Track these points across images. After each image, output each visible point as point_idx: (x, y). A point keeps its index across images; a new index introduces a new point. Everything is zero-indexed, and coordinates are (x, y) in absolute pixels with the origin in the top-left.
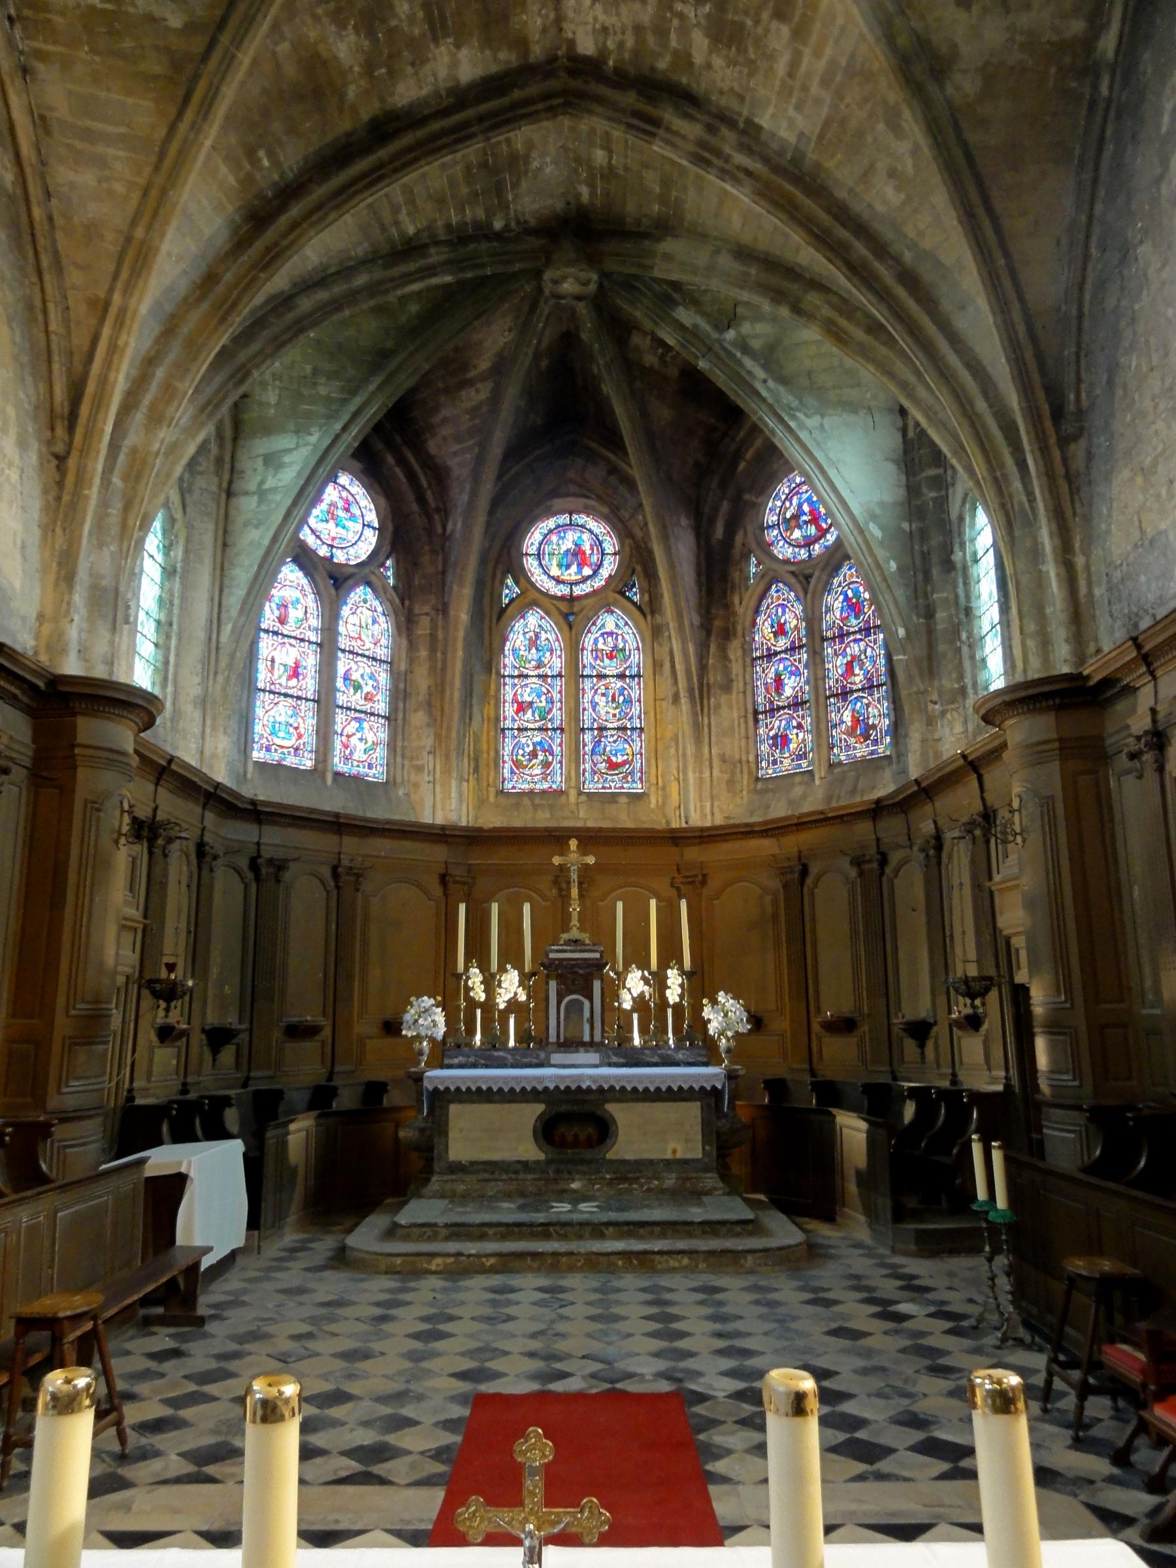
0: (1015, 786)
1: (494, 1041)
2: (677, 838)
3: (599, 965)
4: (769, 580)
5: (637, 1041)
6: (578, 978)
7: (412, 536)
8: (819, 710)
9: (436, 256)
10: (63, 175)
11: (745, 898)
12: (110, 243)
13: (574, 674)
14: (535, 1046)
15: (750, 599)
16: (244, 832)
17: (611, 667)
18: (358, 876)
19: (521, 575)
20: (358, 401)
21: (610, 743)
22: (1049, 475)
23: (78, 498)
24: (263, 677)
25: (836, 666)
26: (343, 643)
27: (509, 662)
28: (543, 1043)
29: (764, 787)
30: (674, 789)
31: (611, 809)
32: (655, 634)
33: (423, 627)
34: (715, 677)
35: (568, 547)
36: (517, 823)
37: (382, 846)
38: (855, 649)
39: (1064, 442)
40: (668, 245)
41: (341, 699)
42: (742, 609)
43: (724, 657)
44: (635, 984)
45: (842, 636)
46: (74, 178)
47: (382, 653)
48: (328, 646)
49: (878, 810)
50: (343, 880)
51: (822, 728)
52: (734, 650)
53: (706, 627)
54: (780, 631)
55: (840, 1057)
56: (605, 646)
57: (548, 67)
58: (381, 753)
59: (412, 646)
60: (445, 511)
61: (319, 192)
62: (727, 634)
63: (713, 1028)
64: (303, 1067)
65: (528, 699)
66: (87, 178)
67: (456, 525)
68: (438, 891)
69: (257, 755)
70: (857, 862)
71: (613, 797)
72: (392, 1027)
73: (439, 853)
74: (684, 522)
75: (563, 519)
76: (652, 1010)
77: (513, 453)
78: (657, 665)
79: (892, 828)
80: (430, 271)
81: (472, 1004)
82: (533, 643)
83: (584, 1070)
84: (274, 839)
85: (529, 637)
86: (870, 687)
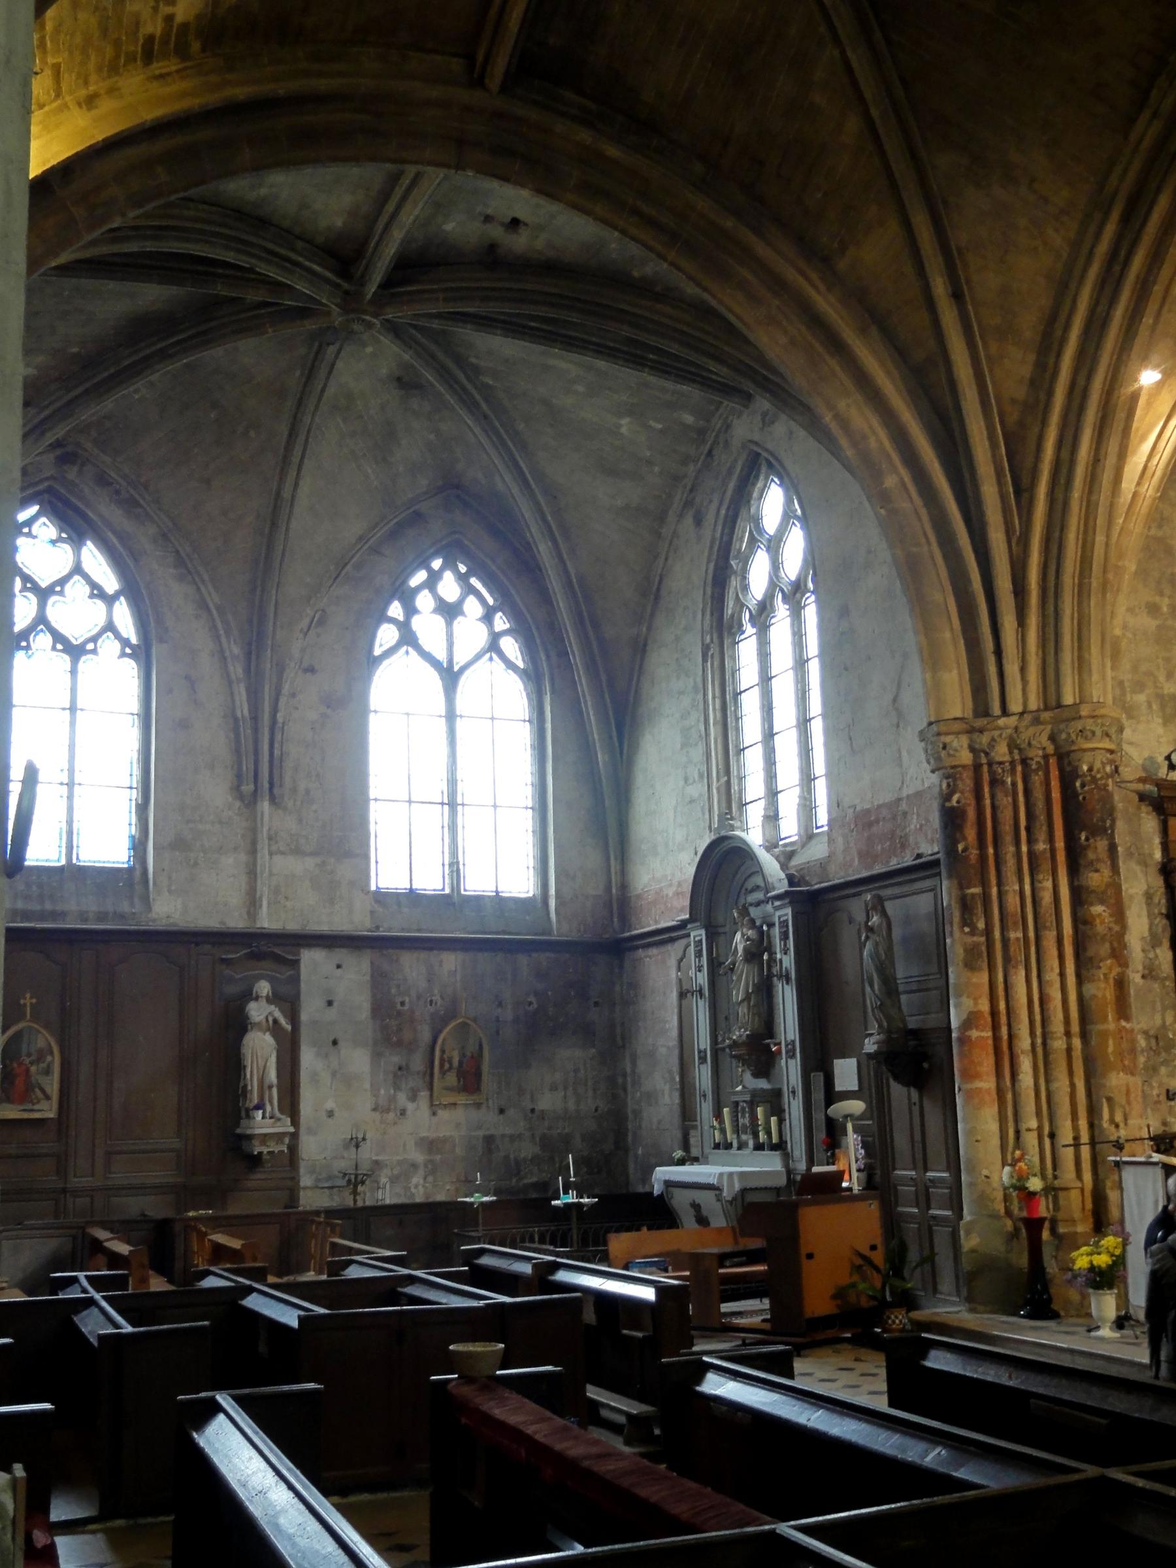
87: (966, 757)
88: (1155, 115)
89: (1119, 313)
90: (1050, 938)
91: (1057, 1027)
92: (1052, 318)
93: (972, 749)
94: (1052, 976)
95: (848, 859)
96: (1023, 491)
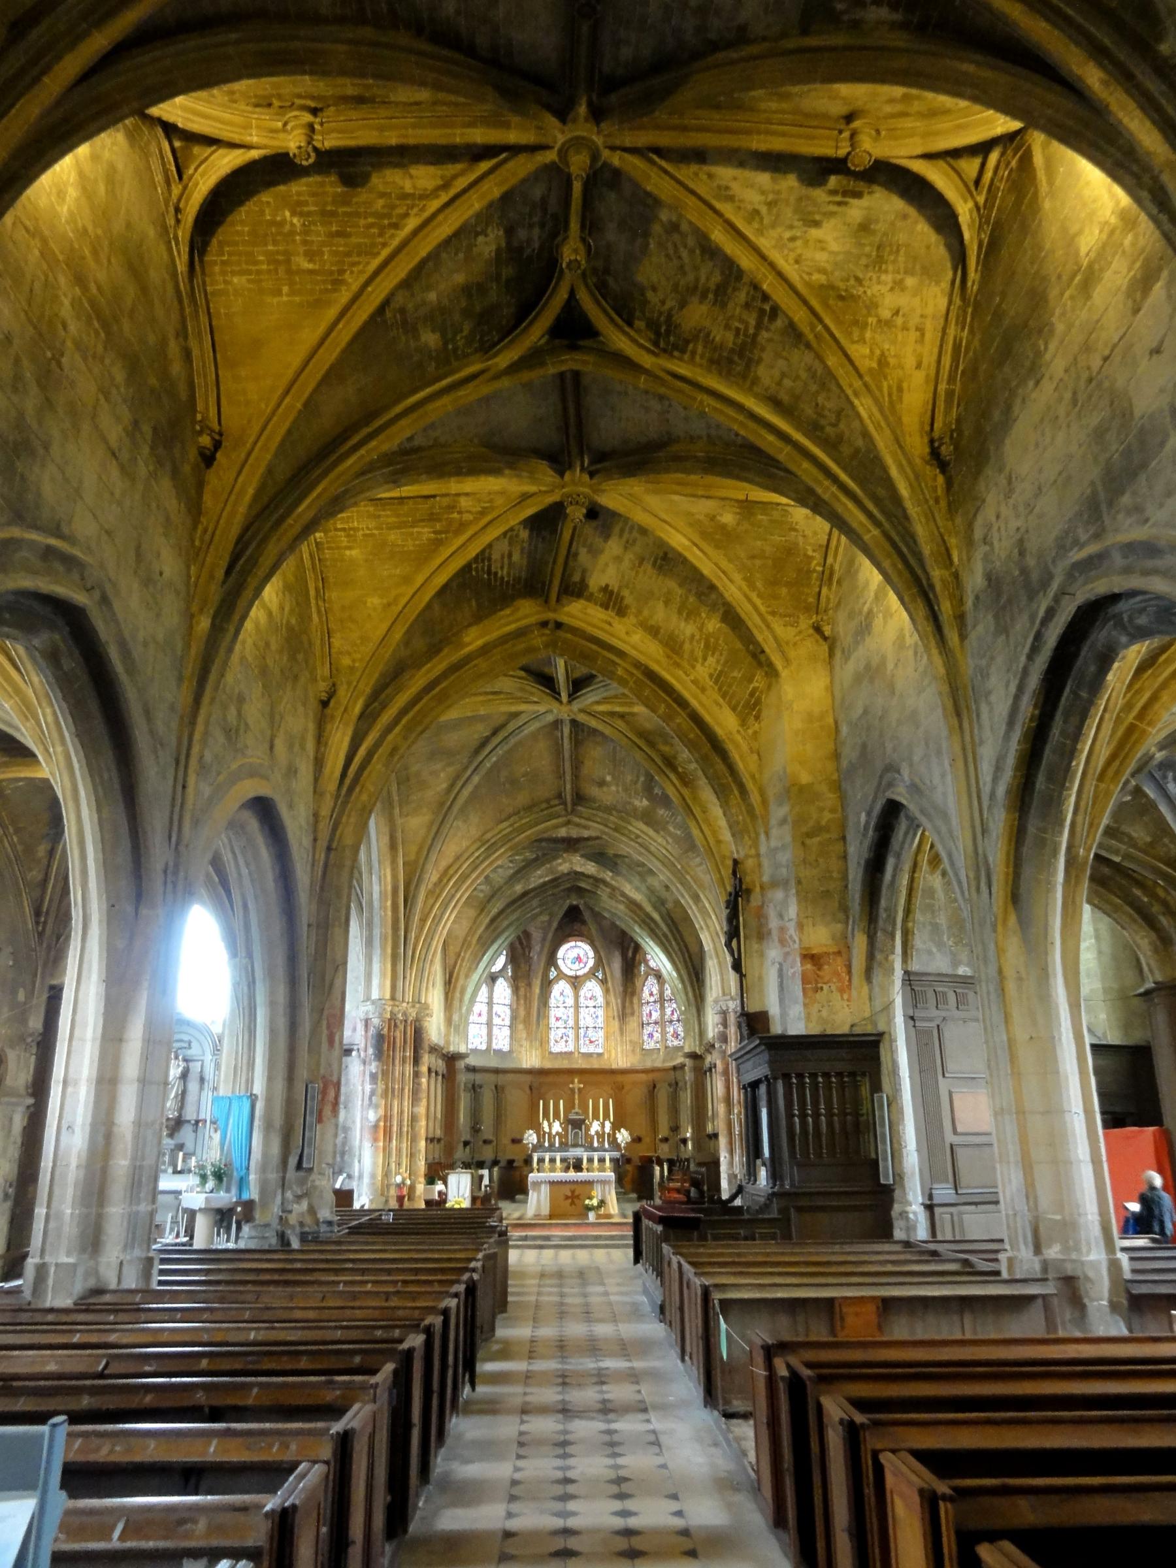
0: (689, 1076)
1: (552, 1145)
2: (613, 1072)
4: (647, 975)
5: (596, 1144)
6: (578, 1124)
7: (519, 956)
8: (660, 1029)
11: (635, 1096)
13: (577, 1006)
14: (564, 1146)
15: (641, 979)
16: (471, 1076)
17: (591, 1003)
18: (503, 1088)
19: (557, 968)
21: (590, 1032)
24: (472, 1018)
25: (668, 1011)
28: (566, 1144)
32: (607, 991)
33: (522, 992)
34: (628, 1011)
35: (575, 955)
37: (510, 1077)
42: (638, 984)
43: (631, 1003)
44: (595, 1127)
47: (508, 1002)
48: (490, 1004)
49: (675, 1068)
51: (664, 1033)
52: (635, 1000)
53: (625, 992)
54: (651, 994)
55: (664, 1151)
62: (633, 993)
67: (534, 954)
71: (590, 1055)
72: (517, 1141)
73: (528, 1078)
75: (573, 944)
76: (600, 1135)
78: (608, 1003)
79: (678, 1073)
85: (560, 991)
89: (474, 876)
96: (423, 921)
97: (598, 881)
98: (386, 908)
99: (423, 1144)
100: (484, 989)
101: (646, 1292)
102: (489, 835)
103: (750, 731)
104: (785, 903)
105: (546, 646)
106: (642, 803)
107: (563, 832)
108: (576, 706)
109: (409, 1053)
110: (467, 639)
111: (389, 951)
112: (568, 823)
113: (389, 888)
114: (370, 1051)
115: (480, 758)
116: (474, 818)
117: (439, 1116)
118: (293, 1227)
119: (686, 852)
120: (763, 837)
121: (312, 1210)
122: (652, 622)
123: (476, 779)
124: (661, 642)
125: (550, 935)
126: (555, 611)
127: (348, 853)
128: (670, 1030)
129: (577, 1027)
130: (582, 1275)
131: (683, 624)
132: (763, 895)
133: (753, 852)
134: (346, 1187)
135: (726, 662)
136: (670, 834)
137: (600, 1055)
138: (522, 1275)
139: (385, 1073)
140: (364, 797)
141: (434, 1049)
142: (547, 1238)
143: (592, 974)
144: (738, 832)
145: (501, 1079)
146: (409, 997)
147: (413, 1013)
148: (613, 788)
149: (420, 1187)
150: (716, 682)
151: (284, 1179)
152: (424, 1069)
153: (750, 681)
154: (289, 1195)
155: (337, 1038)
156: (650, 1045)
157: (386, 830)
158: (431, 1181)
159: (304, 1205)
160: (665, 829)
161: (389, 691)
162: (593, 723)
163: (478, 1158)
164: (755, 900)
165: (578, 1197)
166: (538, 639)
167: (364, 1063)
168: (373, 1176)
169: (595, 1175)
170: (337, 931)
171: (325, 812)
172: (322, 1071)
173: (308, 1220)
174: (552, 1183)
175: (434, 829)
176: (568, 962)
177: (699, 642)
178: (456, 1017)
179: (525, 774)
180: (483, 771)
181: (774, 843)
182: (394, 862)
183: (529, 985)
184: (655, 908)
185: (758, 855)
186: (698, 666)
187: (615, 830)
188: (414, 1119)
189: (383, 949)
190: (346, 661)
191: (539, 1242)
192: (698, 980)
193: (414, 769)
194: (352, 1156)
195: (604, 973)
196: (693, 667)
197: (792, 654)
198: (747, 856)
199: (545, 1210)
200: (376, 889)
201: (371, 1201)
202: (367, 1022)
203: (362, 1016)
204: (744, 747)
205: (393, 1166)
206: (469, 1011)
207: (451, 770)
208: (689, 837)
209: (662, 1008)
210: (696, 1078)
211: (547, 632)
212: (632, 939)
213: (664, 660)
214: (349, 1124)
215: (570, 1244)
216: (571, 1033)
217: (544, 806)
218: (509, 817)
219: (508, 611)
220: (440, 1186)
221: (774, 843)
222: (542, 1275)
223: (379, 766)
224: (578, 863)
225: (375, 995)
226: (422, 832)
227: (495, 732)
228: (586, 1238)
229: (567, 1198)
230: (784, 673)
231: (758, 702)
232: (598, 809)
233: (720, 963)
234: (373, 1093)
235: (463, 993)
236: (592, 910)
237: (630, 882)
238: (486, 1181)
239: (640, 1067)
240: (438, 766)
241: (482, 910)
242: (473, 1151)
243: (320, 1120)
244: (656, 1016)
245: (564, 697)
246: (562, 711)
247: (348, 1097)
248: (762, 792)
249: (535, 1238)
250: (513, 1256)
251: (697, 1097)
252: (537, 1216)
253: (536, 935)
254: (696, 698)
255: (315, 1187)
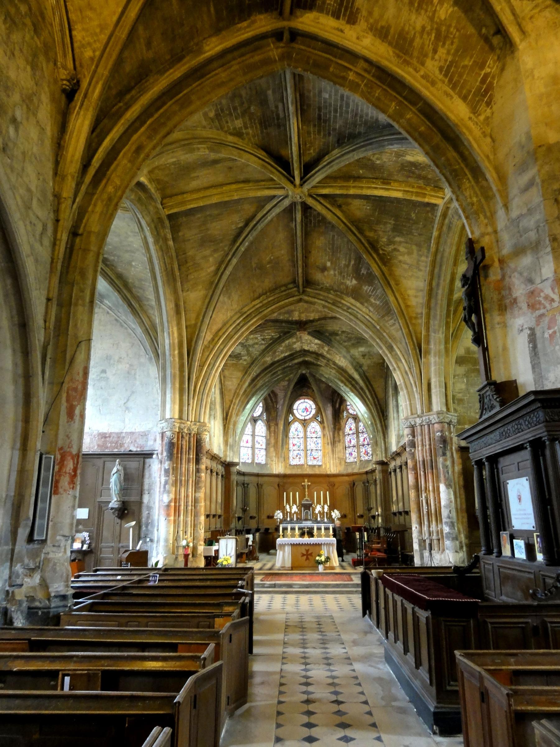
0: (378, 476)
1: (292, 520)
3: (311, 505)
4: (348, 418)
5: (319, 519)
6: (307, 507)
8: (357, 450)
9: (279, 373)
10: (227, 383)
11: (342, 490)
12: (233, 392)
13: (306, 437)
14: (299, 520)
15: (344, 421)
16: (241, 478)
17: (314, 435)
18: (262, 485)
19: (293, 414)
20: (262, 392)
21: (314, 453)
22: (382, 426)
23: (228, 431)
24: (242, 444)
25: (361, 439)
26: (256, 434)
27: (291, 435)
28: (301, 519)
29: (348, 464)
30: (328, 464)
31: (314, 469)
32: (324, 428)
34: (336, 439)
35: (304, 407)
36: (294, 473)
37: (266, 479)
38: (365, 436)
39: (384, 421)
40: (322, 368)
41: (256, 446)
42: (342, 423)
44: (318, 509)
45: (363, 432)
46: (228, 383)
47: (264, 435)
48: (253, 435)
49: (367, 473)
50: (259, 486)
51: (359, 452)
52: (341, 433)
53: (335, 428)
54: (351, 429)
55: (361, 523)
56: (313, 430)
57: (300, 351)
58: (264, 458)
59: (270, 433)
60: (277, 402)
61: (262, 375)
62: (339, 429)
63: (333, 517)
64: (253, 525)
65: (295, 443)
66: (230, 383)
67: (279, 406)
68: (277, 487)
69: (241, 461)
70: (364, 483)
71: (314, 466)
72: (271, 517)
73: (277, 480)
74: (329, 405)
75: (302, 401)
76: (322, 514)
77: (292, 393)
78: (324, 435)
79: (369, 476)
80: (278, 375)
81: (287, 512)
82: (296, 430)
83: (309, 524)
84: (247, 479)
85: (295, 428)
86: (368, 445)
87: (177, 430)
88: (261, 302)
89: (236, 337)
90: (191, 480)
91: (190, 503)
92: (220, 330)
93: (179, 428)
94: (190, 490)
95: (91, 446)
96: (201, 366)
97: (318, 355)
98: (174, 356)
99: (202, 518)
100: (249, 426)
101: (388, 659)
102: (246, 309)
103: (482, 118)
104: (536, 267)
105: (282, 57)
106: (352, 283)
107: (296, 316)
108: (306, 187)
109: (192, 456)
110: (207, 48)
111: (177, 385)
112: (300, 300)
113: (176, 341)
114: (165, 454)
115: (238, 244)
116: (235, 297)
117: (219, 500)
118: (20, 603)
119: (383, 317)
120: (501, 213)
121: (44, 585)
122: (383, 23)
123: (235, 261)
124: (390, 44)
125: (289, 393)
126: (289, 20)
127: (93, 239)
128: (363, 450)
129: (306, 450)
130: (319, 624)
131: (413, 17)
132: (502, 269)
133: (490, 229)
134: (144, 549)
135: (457, 51)
136: (372, 305)
137: (320, 466)
138: (271, 626)
139: (175, 470)
140: (110, 189)
141: (214, 457)
142: (290, 586)
143: (315, 418)
144: (471, 214)
145: (261, 480)
146: (192, 417)
147: (195, 429)
148: (332, 272)
149: (201, 548)
150: (446, 75)
151: (13, 551)
152: (203, 467)
153: (482, 67)
154: (18, 568)
155: (77, 412)
156: (350, 459)
157: (171, 297)
158: (210, 542)
159: (37, 578)
160: (367, 301)
161: (133, 92)
162: (319, 208)
163: (247, 527)
164: (494, 275)
165: (311, 554)
166: (274, 51)
167: (161, 462)
168: (167, 540)
169: (323, 539)
170: (81, 311)
171: (67, 192)
172: (60, 443)
173: (40, 595)
174: (293, 545)
175: (207, 300)
176: (300, 411)
177: (429, 34)
178: (230, 440)
179: (270, 262)
180: (239, 254)
181: (514, 214)
182: (179, 324)
183: (277, 425)
184: (356, 370)
185: (495, 232)
186: (429, 63)
187: (333, 304)
188: (196, 501)
189: (173, 384)
190: (88, 53)
191: (284, 589)
192: (383, 415)
193: (190, 253)
194: (153, 526)
195: (322, 418)
196: (423, 64)
197: (529, 27)
198: (483, 235)
199: (288, 564)
200: (167, 341)
201: (165, 558)
202: (163, 434)
203: (160, 430)
204: (477, 132)
205: (181, 533)
206: (240, 439)
207: (218, 256)
208: (387, 303)
209: (358, 437)
210: (384, 478)
211: (282, 45)
212: (339, 394)
213: (394, 59)
214: (151, 504)
215: (306, 590)
216: (302, 453)
217: (283, 289)
218: (258, 298)
219: (245, 24)
220: (215, 547)
221: (514, 214)
222: (287, 627)
223: (125, 161)
224: (307, 342)
225: (168, 416)
226: (199, 303)
227: (246, 225)
228: (318, 586)
229: (303, 555)
230: (521, 46)
231: (490, 87)
232: (321, 289)
233: (408, 392)
234: (166, 483)
235: (235, 424)
236: (314, 376)
237: (340, 353)
238: (250, 543)
239: (345, 472)
240: (208, 252)
241: (246, 373)
242: (244, 523)
243: (55, 490)
244: (354, 442)
245: (297, 181)
246: (295, 193)
247: (150, 485)
248: (497, 169)
249: (281, 586)
250: (262, 603)
251: (384, 489)
252: (283, 568)
253: (281, 395)
254: (427, 89)
255: (47, 560)
